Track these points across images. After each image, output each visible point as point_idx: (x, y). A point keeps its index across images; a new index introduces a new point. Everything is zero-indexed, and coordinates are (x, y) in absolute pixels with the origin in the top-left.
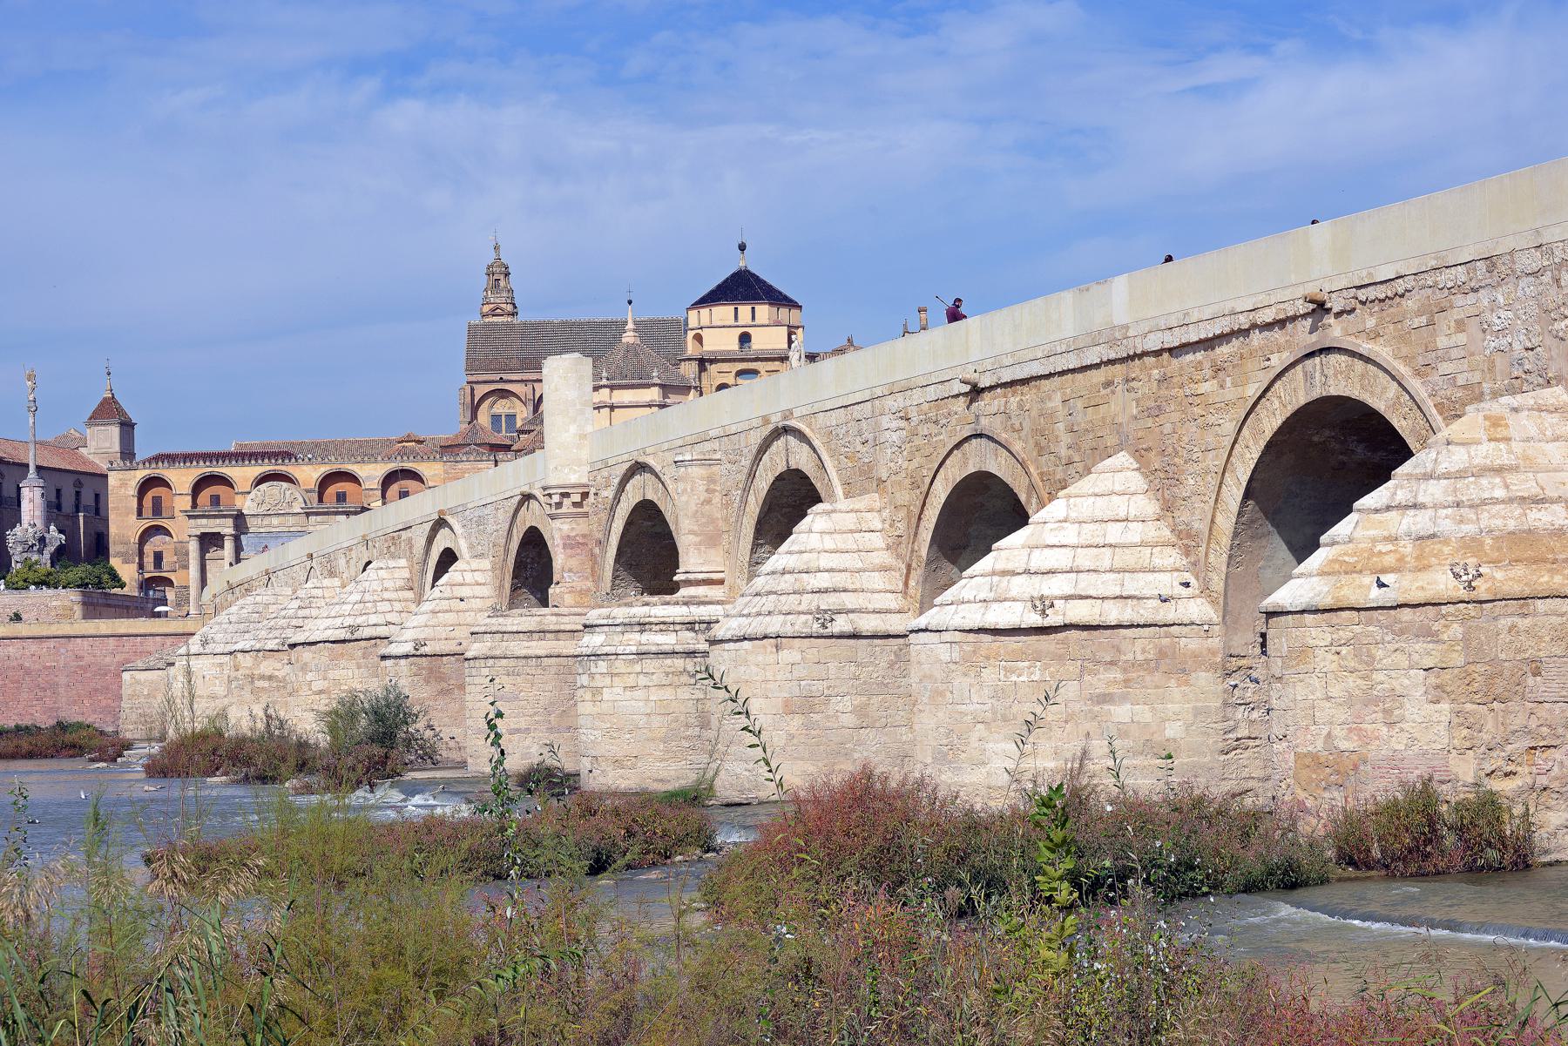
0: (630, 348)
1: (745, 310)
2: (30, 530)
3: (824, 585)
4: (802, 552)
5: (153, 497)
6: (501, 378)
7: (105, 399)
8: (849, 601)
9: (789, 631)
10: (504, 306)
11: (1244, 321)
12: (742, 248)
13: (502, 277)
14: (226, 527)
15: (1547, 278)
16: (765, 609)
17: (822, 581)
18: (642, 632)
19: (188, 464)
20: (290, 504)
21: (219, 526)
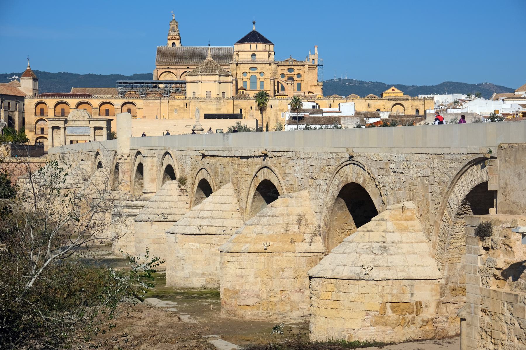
0: (209, 62)
1: (254, 45)
3: (166, 206)
4: (161, 195)
6: (168, 68)
7: (27, 70)
8: (172, 211)
9: (155, 219)
10: (175, 36)
11: (253, 154)
12: (254, 23)
13: (175, 26)
14: (61, 124)
15: (305, 161)
16: (148, 213)
17: (166, 205)
18: (129, 208)
20: (84, 117)
21: (58, 124)
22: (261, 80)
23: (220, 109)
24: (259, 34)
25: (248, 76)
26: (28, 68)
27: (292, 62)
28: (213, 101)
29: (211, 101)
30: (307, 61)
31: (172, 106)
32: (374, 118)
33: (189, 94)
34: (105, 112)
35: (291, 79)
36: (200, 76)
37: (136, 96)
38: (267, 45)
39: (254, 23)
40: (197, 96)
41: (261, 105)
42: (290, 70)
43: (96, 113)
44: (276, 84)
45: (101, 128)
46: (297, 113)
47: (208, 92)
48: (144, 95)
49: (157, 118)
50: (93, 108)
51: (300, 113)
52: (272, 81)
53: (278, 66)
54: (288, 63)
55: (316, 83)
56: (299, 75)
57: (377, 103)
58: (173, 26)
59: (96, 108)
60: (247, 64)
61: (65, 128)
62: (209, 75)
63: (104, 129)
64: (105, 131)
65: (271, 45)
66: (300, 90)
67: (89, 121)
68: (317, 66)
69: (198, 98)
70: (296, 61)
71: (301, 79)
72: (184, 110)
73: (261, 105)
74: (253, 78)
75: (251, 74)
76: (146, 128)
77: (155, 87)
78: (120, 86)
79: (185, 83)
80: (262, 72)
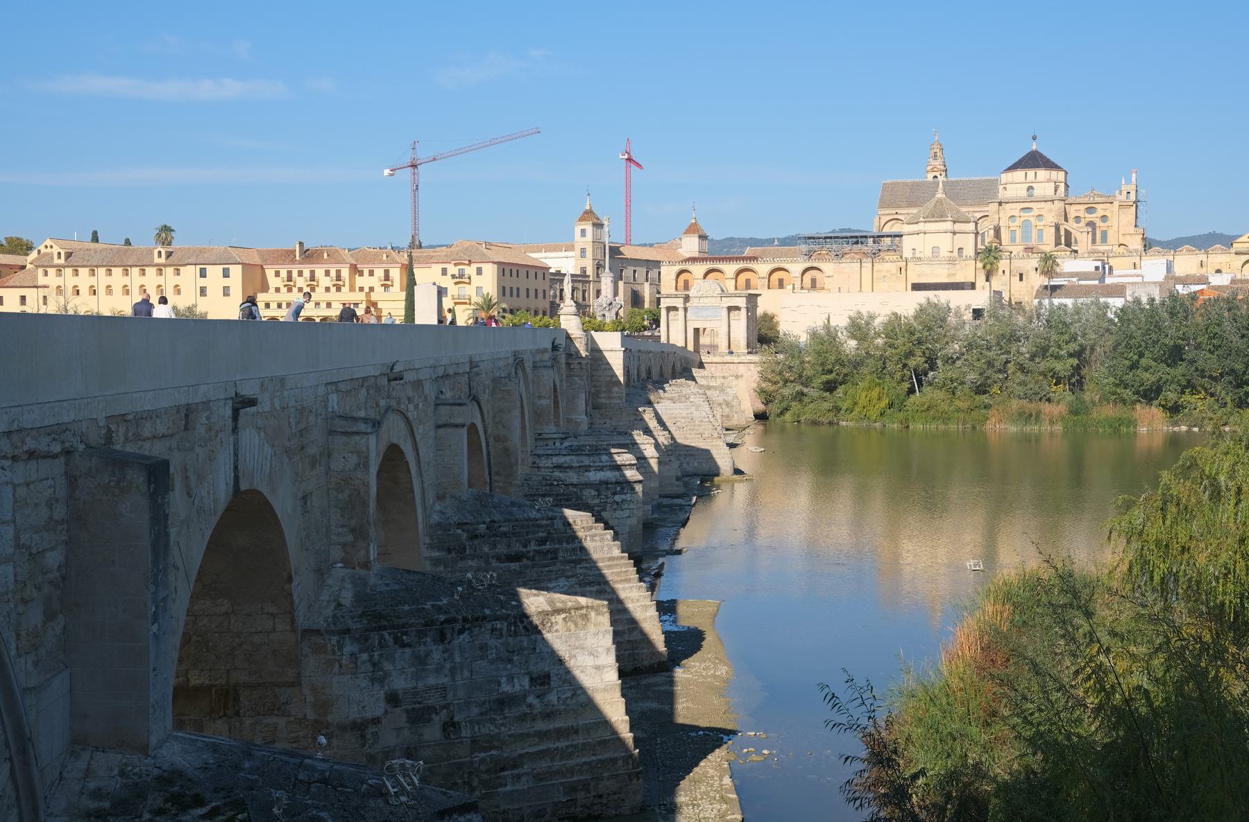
0: (940, 201)
1: (1031, 173)
2: (604, 299)
5: (685, 280)
7: (692, 224)
10: (938, 167)
13: (938, 150)
14: (679, 303)
19: (701, 263)
20: (714, 292)
22: (1038, 228)
23: (954, 275)
24: (1042, 156)
25: (1018, 222)
26: (693, 221)
27: (1094, 198)
28: (942, 262)
29: (939, 262)
30: (1117, 195)
31: (878, 271)
32: (1198, 284)
33: (907, 253)
34: (777, 283)
35: (1091, 224)
36: (923, 223)
37: (827, 257)
38: (1052, 172)
39: (1034, 138)
40: (918, 255)
41: (988, 267)
42: (1090, 210)
43: (763, 285)
44: (1062, 233)
45: (737, 308)
46: (1049, 278)
47: (935, 250)
48: (839, 256)
49: (840, 291)
50: (759, 278)
51: (1054, 279)
52: (1053, 229)
53: (1071, 204)
54: (1086, 200)
55: (1132, 229)
56: (1104, 218)
57: (1218, 258)
58: (935, 151)
59: (763, 278)
60: (1017, 202)
61: (686, 309)
62: (936, 221)
63: (742, 309)
64: (744, 312)
65: (1059, 172)
66: (1106, 242)
67: (721, 297)
68: (1134, 203)
69: (920, 259)
70: (1101, 196)
71: (1108, 224)
72: (897, 278)
73: (988, 267)
74: (1026, 226)
75: (1022, 219)
76: (819, 306)
77: (857, 243)
78: (806, 243)
79: (902, 236)
80: (1104, 216)
